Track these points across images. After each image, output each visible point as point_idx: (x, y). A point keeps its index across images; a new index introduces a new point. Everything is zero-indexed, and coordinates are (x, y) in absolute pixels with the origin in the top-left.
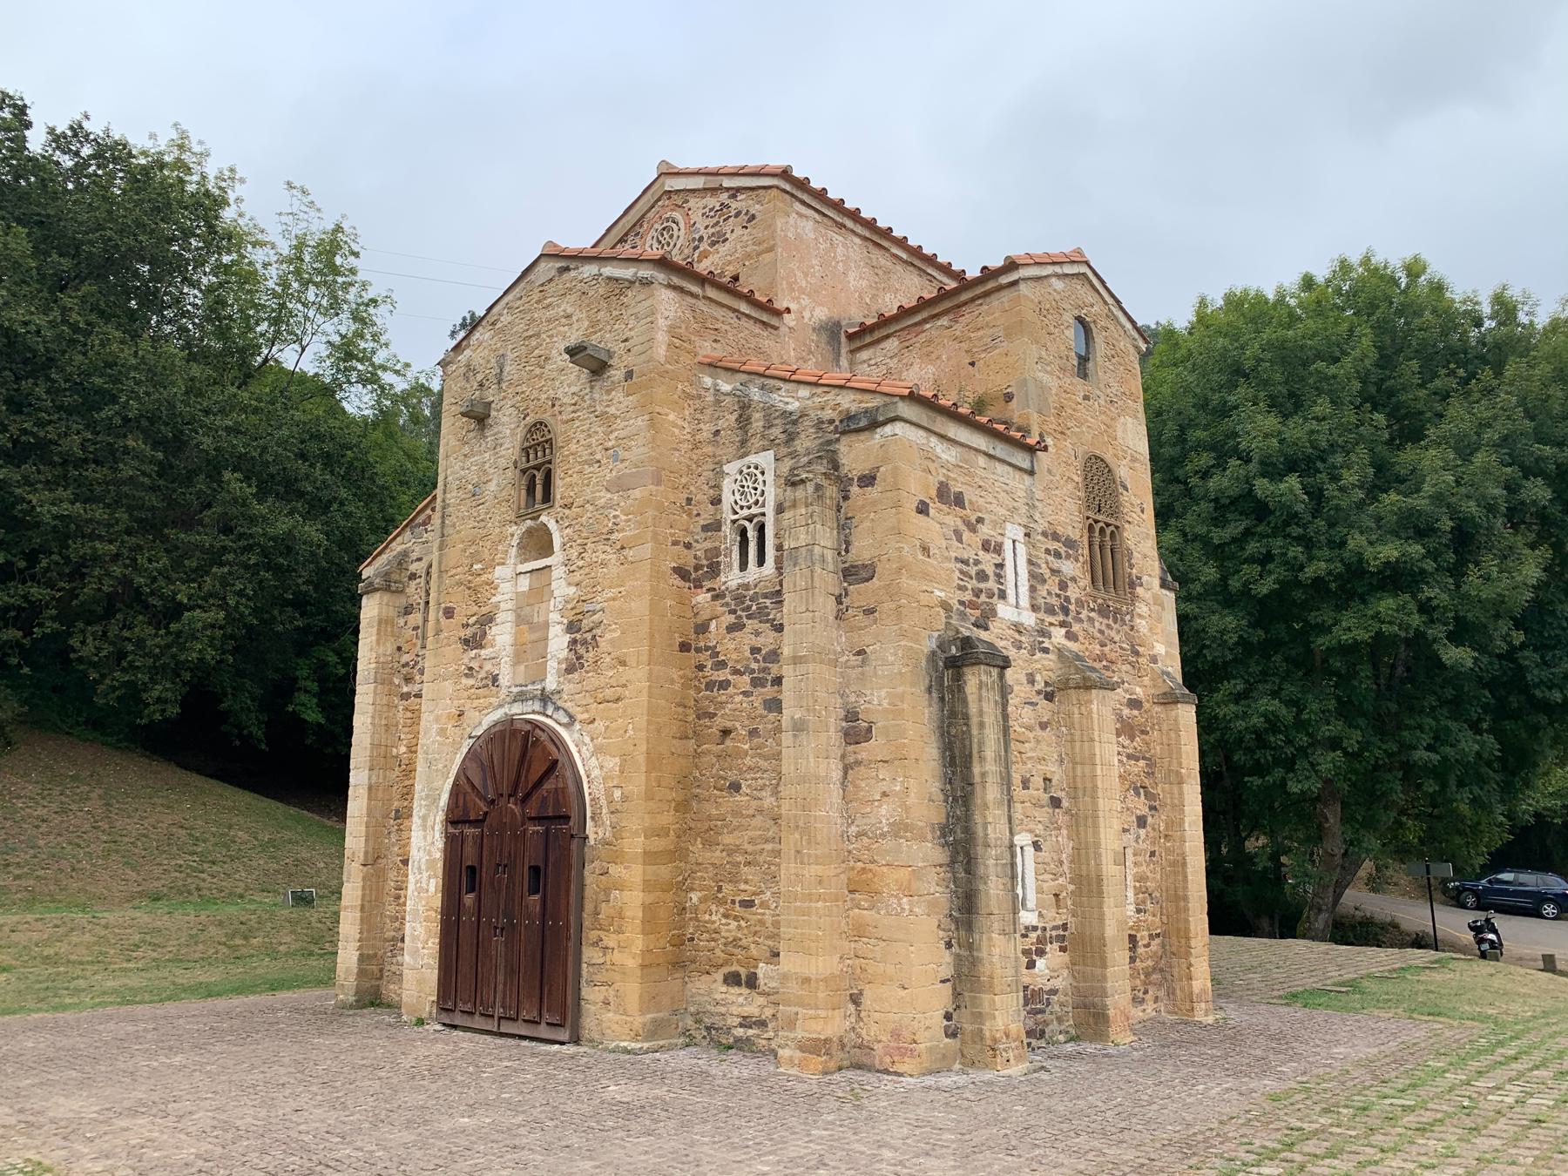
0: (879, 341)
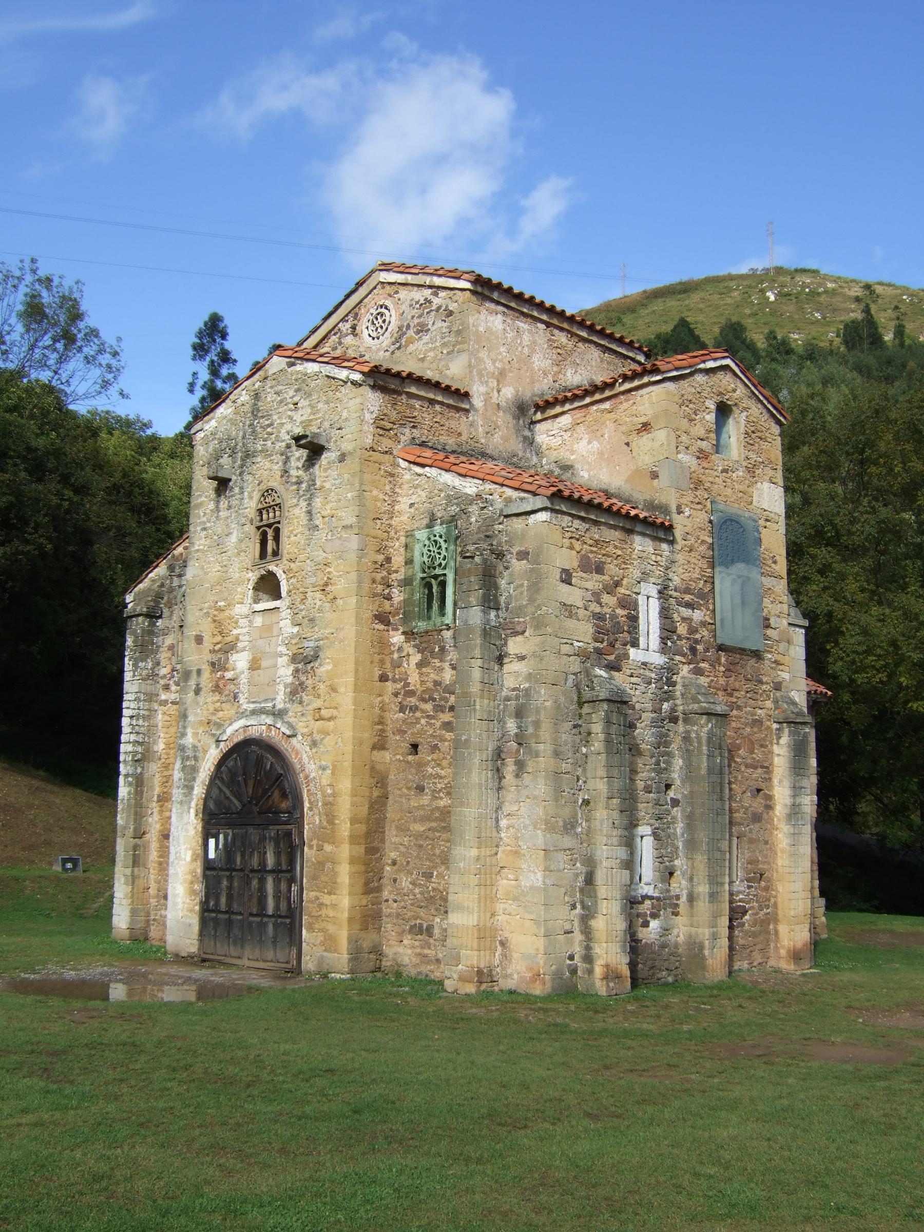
0: (556, 416)
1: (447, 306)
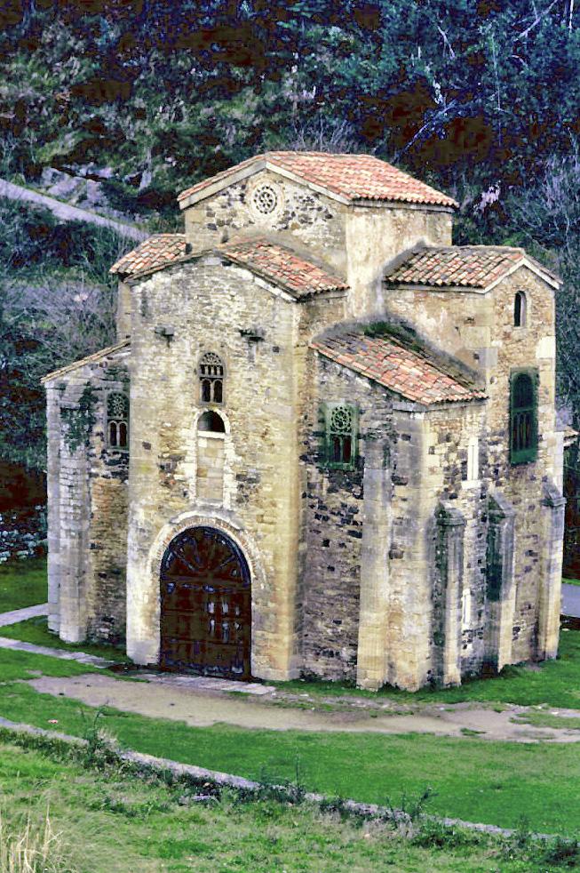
1: (326, 211)
